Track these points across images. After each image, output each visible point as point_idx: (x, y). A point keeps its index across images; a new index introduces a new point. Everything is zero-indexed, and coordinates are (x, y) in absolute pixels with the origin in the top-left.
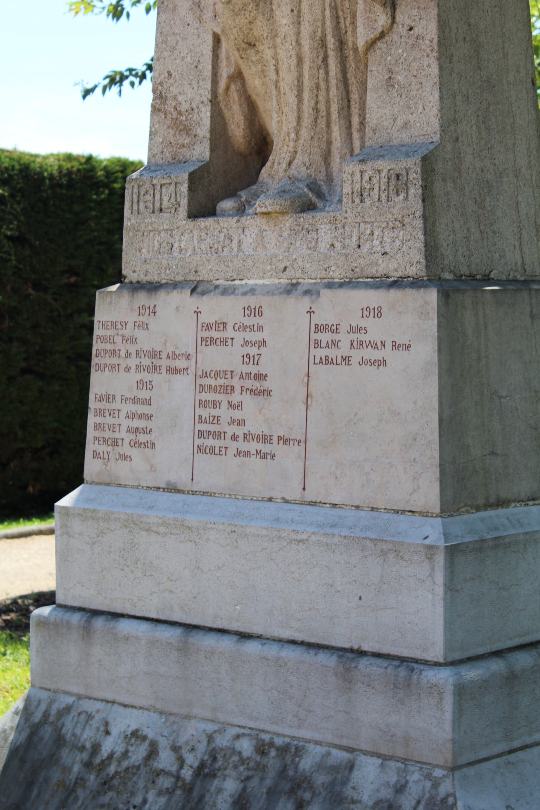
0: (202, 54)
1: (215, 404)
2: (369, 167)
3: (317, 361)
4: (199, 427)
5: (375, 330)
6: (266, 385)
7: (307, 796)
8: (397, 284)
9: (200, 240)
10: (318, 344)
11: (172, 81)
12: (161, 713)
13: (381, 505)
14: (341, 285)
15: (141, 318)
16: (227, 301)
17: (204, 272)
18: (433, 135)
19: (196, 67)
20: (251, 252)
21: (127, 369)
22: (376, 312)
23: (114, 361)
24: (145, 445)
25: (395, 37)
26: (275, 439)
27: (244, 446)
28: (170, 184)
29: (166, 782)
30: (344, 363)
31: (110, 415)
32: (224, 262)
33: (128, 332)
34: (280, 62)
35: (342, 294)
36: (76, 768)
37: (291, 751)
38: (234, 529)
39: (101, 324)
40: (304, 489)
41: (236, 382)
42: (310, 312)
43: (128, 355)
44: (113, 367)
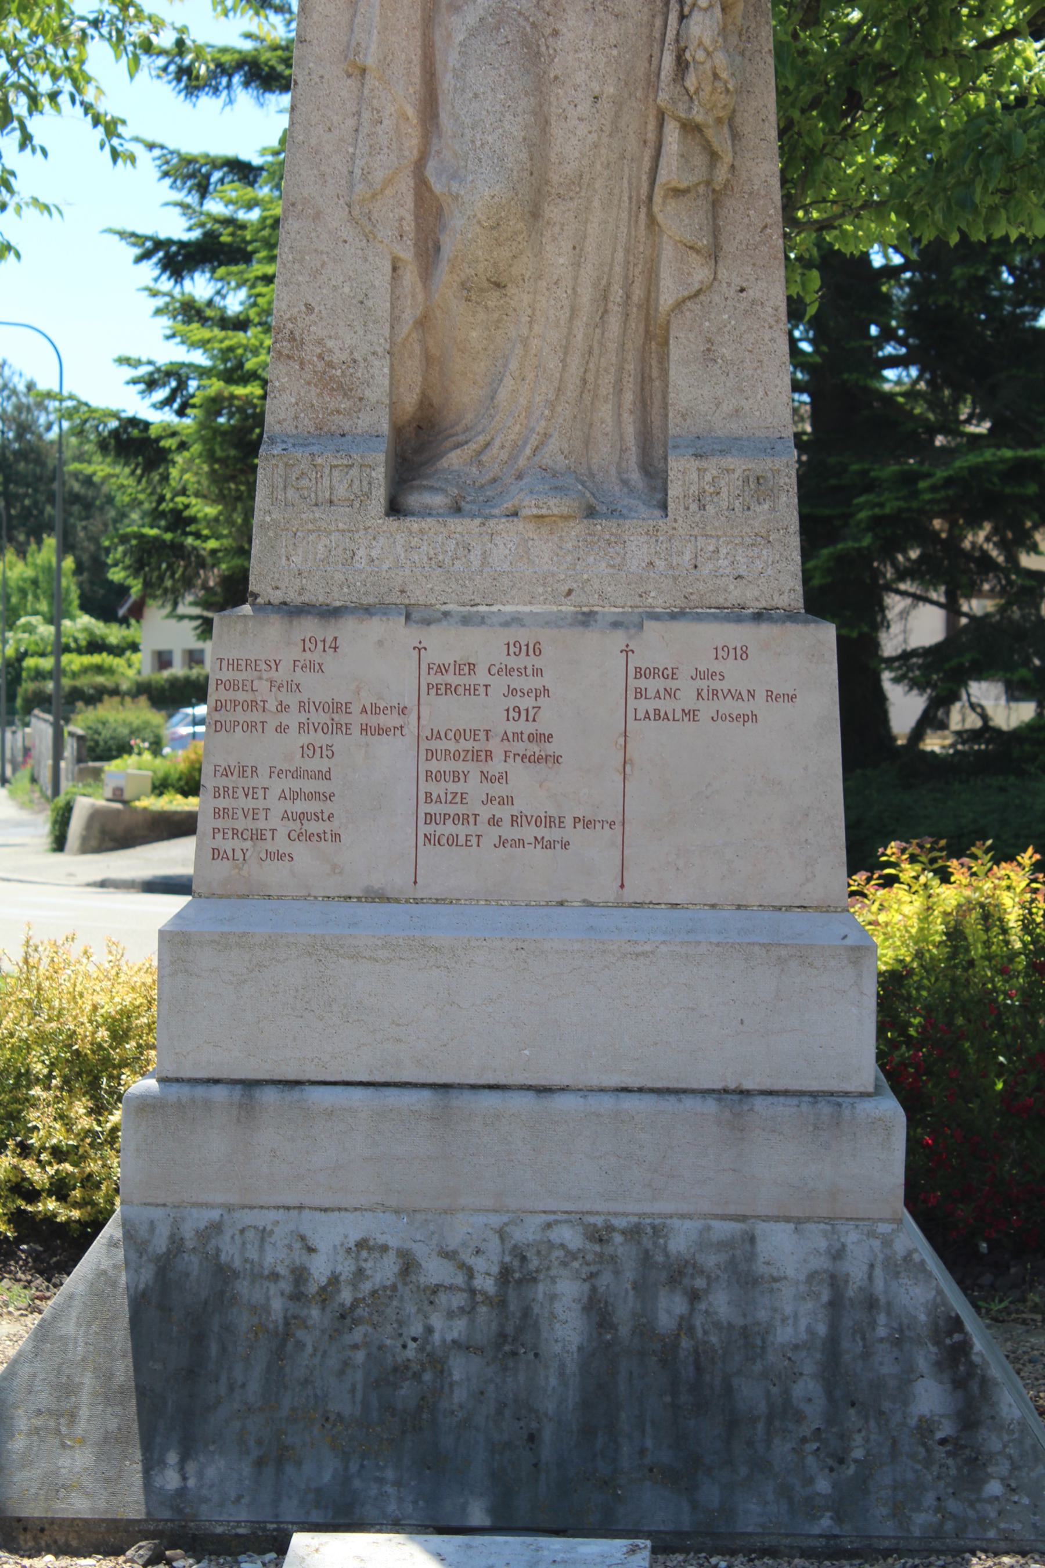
0: (373, 286)
1: (456, 777)
2: (712, 466)
3: (641, 715)
4: (424, 808)
5: (736, 675)
6: (550, 748)
7: (700, 1283)
8: (758, 617)
9: (409, 548)
11: (313, 317)
12: (397, 1212)
13: (754, 901)
14: (673, 617)
15: (308, 655)
16: (474, 635)
17: (418, 592)
18: (782, 429)
19: (362, 303)
20: (506, 567)
21: (281, 729)
22: (739, 652)
23: (256, 716)
25: (716, 299)
26: (569, 822)
28: (352, 466)
29: (459, 1300)
30: (686, 719)
31: (247, 795)
32: (457, 580)
33: (282, 674)
34: (538, 313)
35: (679, 627)
36: (277, 1305)
37: (644, 1234)
38: (520, 945)
39: (225, 663)
40: (622, 886)
41: (495, 746)
42: (627, 651)
43: (283, 708)
44: (251, 726)
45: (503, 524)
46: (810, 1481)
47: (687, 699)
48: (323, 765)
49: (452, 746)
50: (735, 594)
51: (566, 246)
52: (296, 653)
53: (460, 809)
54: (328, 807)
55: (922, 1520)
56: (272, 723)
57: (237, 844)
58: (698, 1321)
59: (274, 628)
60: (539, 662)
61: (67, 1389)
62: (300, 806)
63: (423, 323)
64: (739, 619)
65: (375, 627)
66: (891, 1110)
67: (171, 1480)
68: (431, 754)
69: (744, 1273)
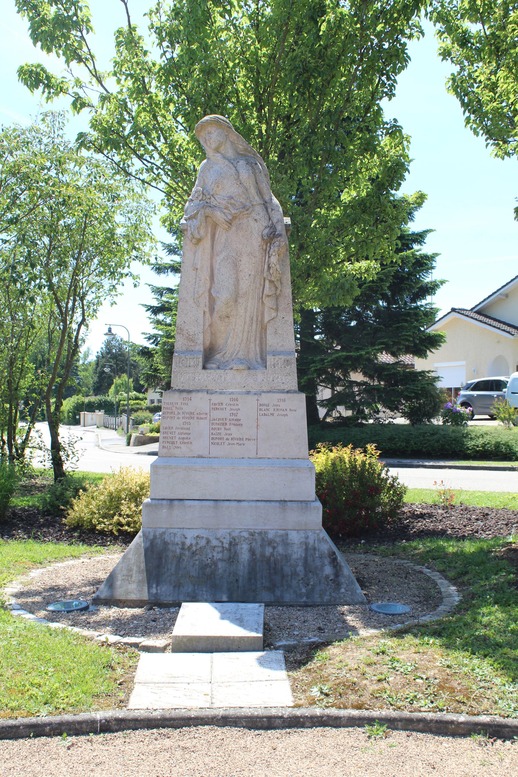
2: (277, 358)
4: (211, 436)
5: (283, 405)
6: (240, 422)
7: (275, 545)
8: (288, 392)
9: (208, 377)
10: (261, 410)
12: (206, 529)
14: (268, 392)
21: (178, 418)
23: (172, 415)
27: (232, 442)
29: (220, 549)
33: (178, 406)
36: (178, 551)
41: (227, 422)
43: (179, 413)
44: (172, 417)
45: (229, 371)
46: (301, 590)
47: (271, 411)
48: (188, 426)
49: (218, 422)
50: (282, 387)
51: (243, 308)
52: (182, 401)
53: (220, 436)
54: (189, 436)
55: (326, 598)
56: (176, 417)
57: (168, 445)
58: (275, 554)
59: (177, 395)
60: (237, 403)
61: (130, 570)
62: (183, 436)
63: (211, 325)
64: (283, 393)
65: (200, 395)
66: (319, 505)
67: (154, 591)
68: (213, 424)
69: (285, 542)
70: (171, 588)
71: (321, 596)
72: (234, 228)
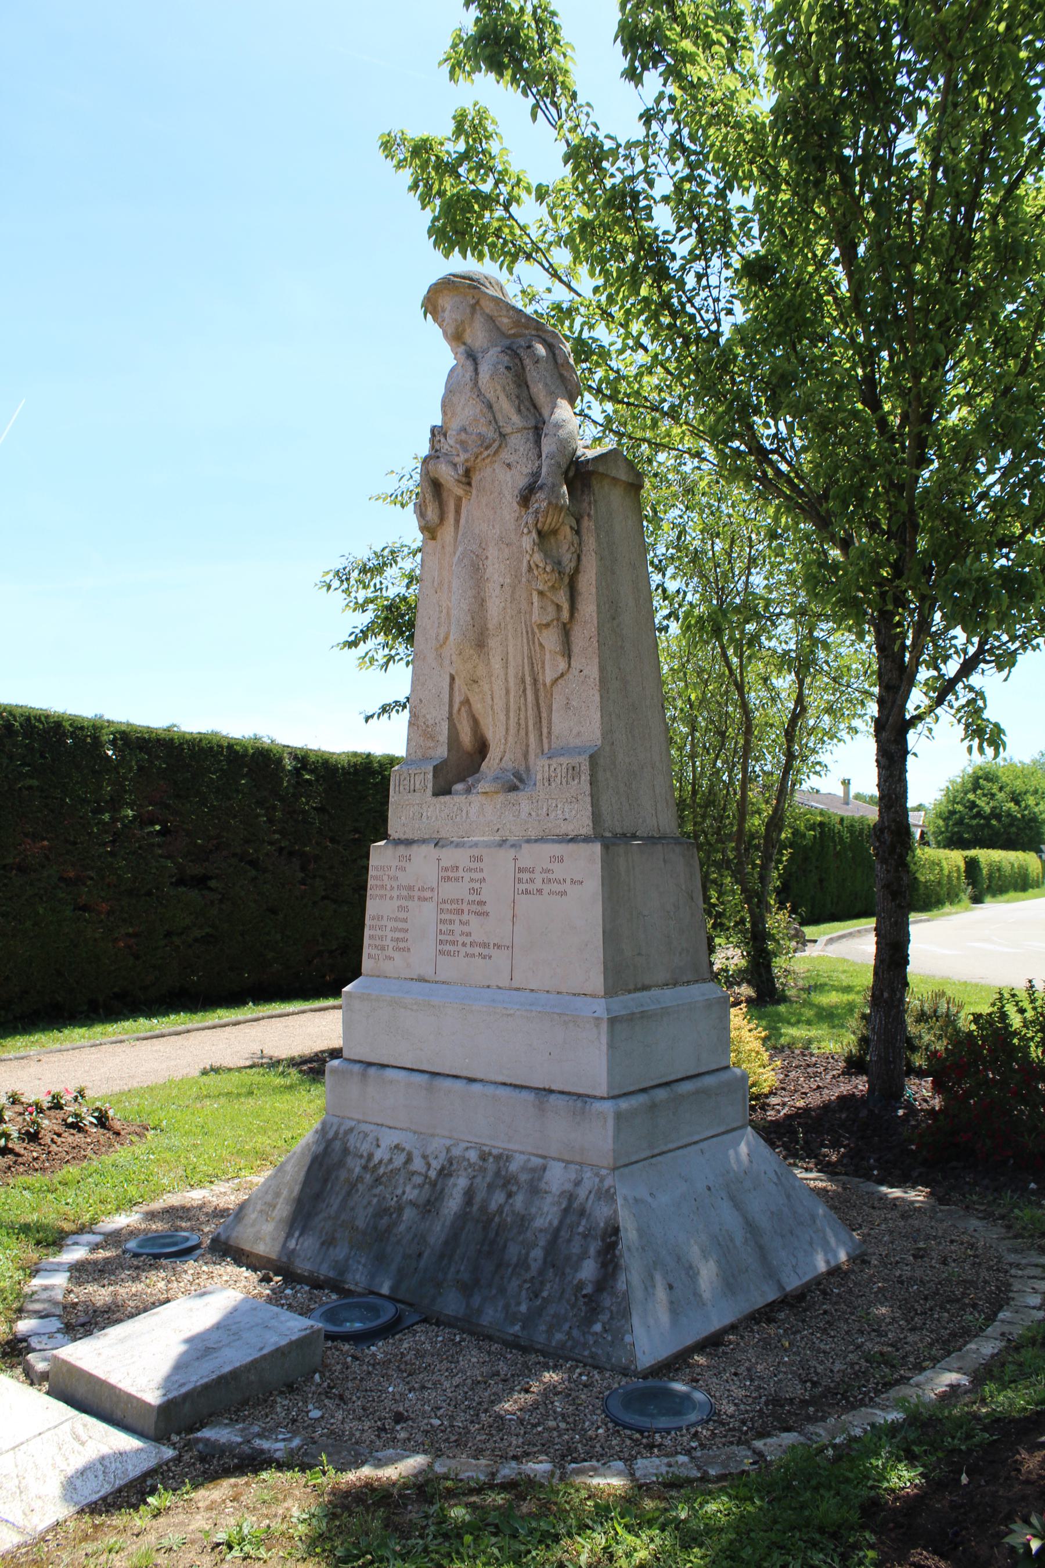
1: (451, 922)
2: (554, 763)
4: (440, 937)
5: (559, 871)
6: (485, 908)
7: (514, 1189)
9: (441, 811)
10: (520, 881)
14: (536, 841)
21: (391, 898)
23: (383, 892)
24: (404, 949)
29: (419, 1180)
33: (392, 873)
36: (357, 1170)
37: (503, 1158)
41: (465, 907)
42: (515, 859)
44: (382, 897)
46: (519, 1304)
47: (538, 884)
49: (449, 907)
51: (498, 658)
58: (506, 1209)
64: (560, 842)
67: (292, 1244)
70: (318, 1246)
71: (550, 1332)
72: (474, 492)
